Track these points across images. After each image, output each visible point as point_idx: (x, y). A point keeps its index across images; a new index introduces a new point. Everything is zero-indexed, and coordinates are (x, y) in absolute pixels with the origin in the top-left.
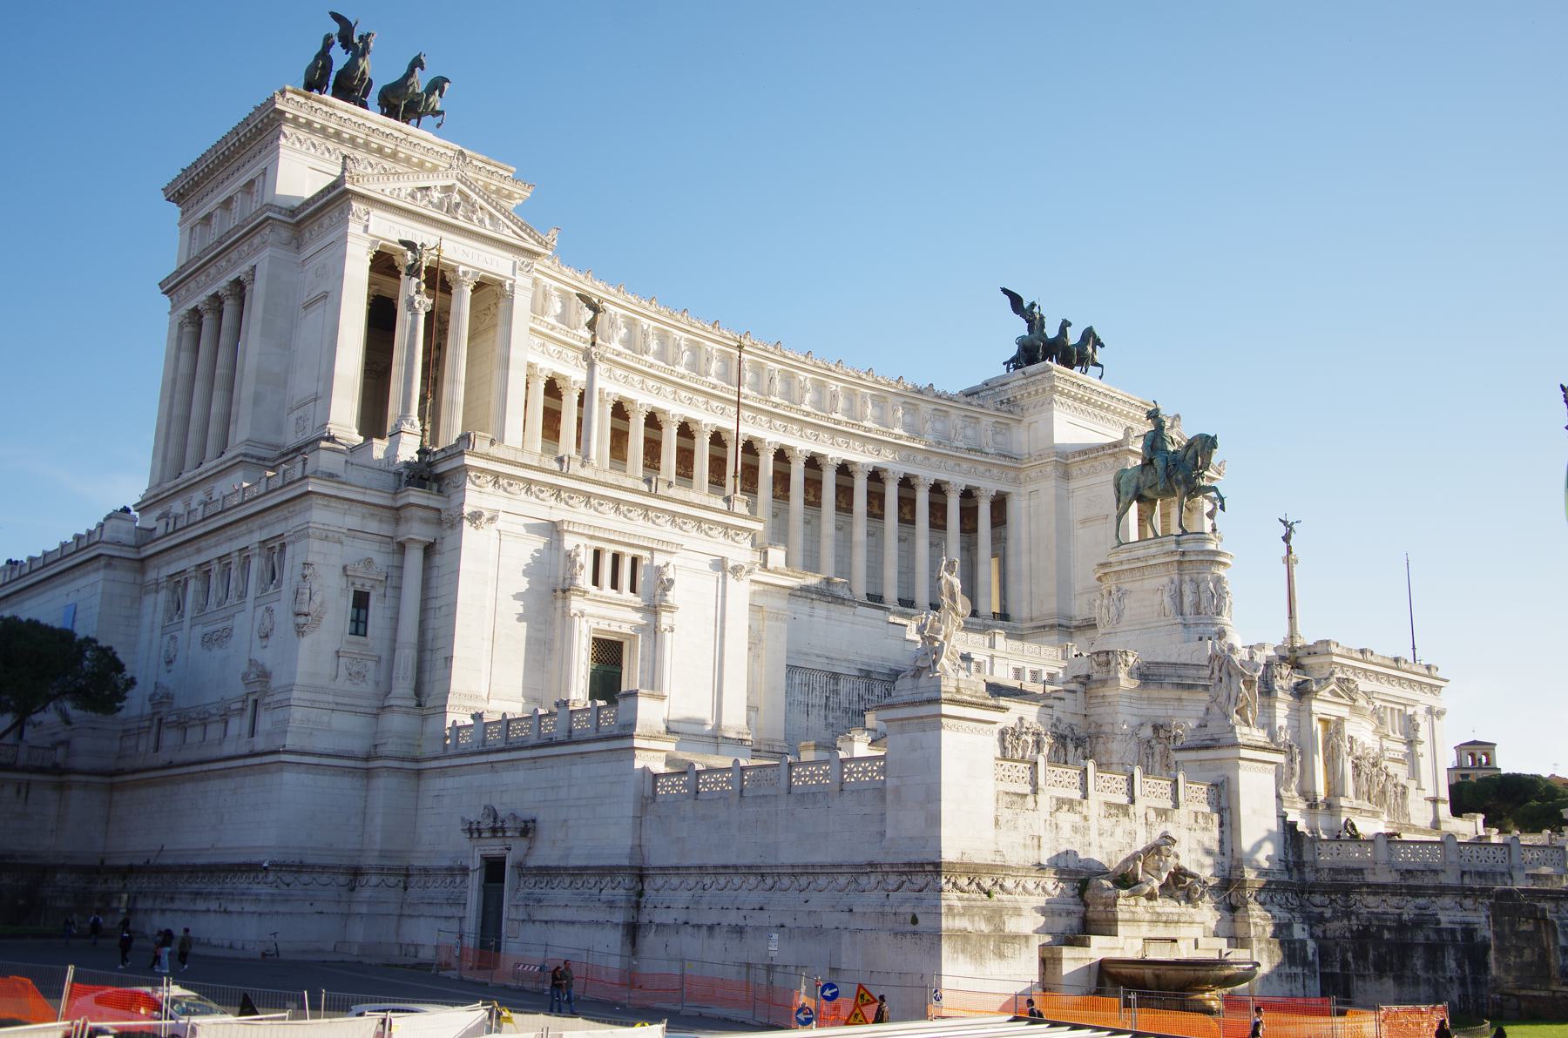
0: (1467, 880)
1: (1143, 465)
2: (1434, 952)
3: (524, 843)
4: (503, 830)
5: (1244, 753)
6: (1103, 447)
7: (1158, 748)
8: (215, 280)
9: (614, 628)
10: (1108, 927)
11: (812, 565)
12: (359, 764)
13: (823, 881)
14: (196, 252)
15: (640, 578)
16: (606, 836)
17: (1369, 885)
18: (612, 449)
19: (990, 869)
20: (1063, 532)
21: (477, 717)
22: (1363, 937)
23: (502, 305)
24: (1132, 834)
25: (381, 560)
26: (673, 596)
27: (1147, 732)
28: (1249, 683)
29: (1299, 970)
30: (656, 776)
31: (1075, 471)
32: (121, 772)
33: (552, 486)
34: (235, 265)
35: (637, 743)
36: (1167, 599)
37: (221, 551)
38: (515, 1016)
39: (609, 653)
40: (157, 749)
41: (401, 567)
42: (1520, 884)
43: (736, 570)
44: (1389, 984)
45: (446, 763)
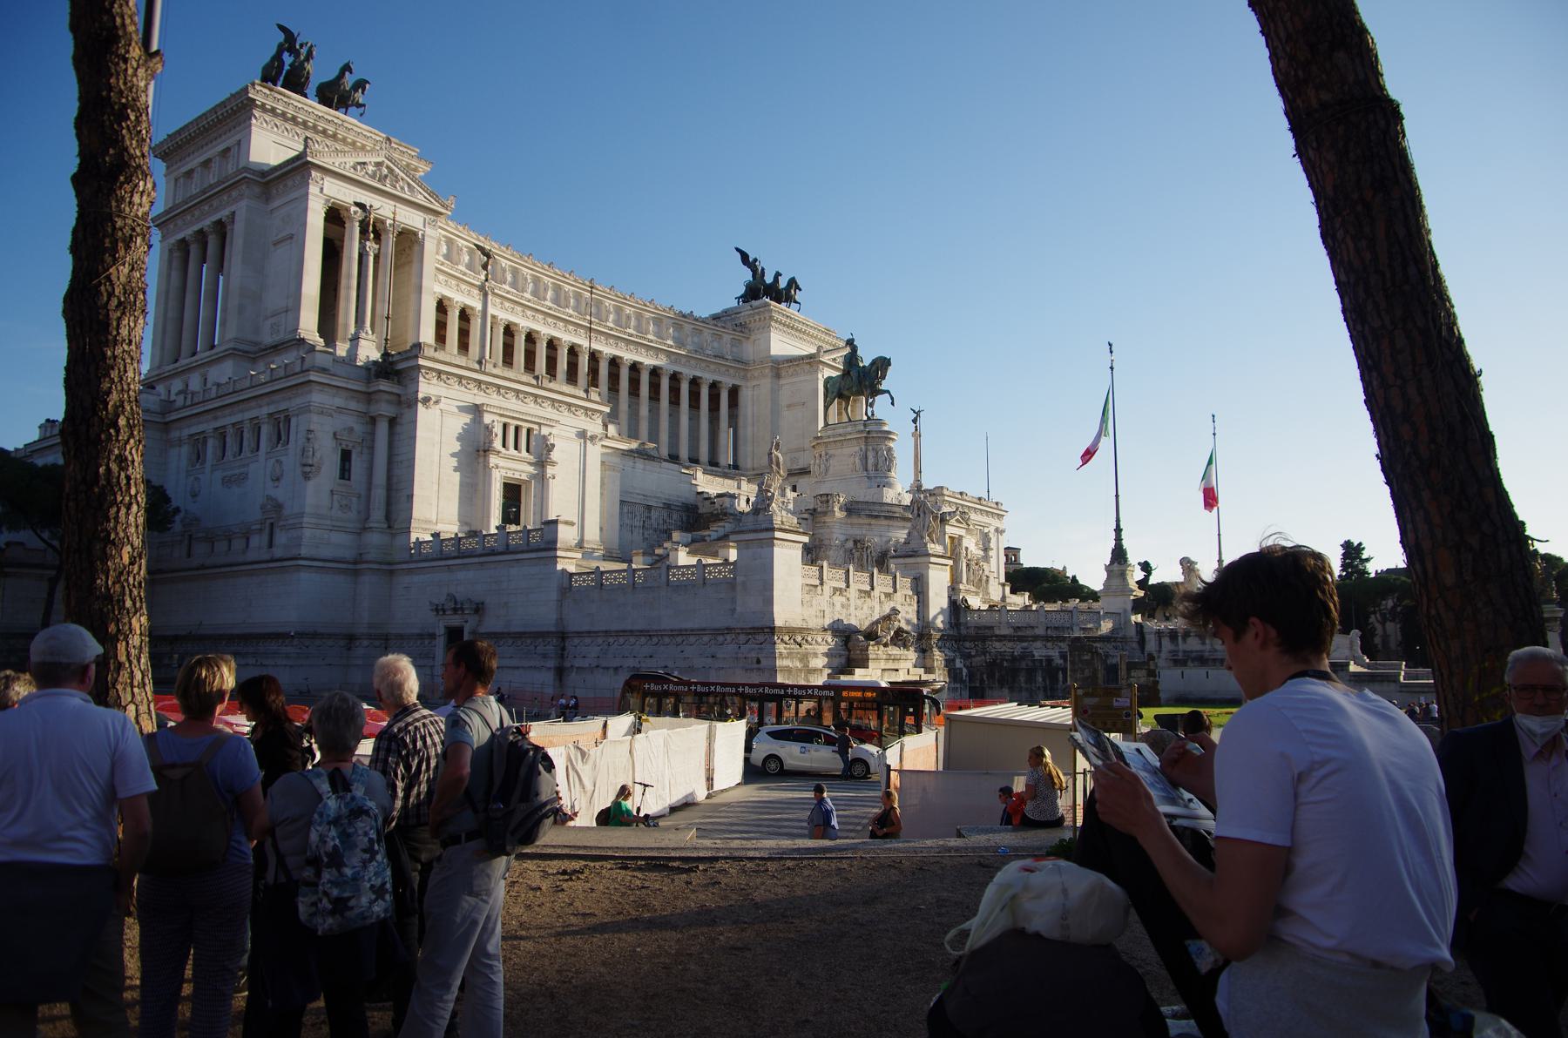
2: (1031, 673)
3: (476, 617)
4: (462, 609)
5: (933, 559)
6: (802, 358)
7: (857, 555)
9: (517, 476)
10: (864, 664)
11: (633, 434)
13: (692, 639)
15: (533, 443)
16: (540, 611)
19: (801, 630)
20: (775, 412)
21: (436, 535)
22: (993, 665)
23: (416, 248)
24: (872, 608)
25: (359, 428)
26: (554, 455)
27: (850, 544)
28: (935, 518)
30: (572, 575)
31: (783, 373)
33: (475, 380)
34: (217, 210)
35: (559, 553)
37: (234, 419)
39: (513, 492)
40: (189, 556)
43: (593, 438)
44: (1006, 691)
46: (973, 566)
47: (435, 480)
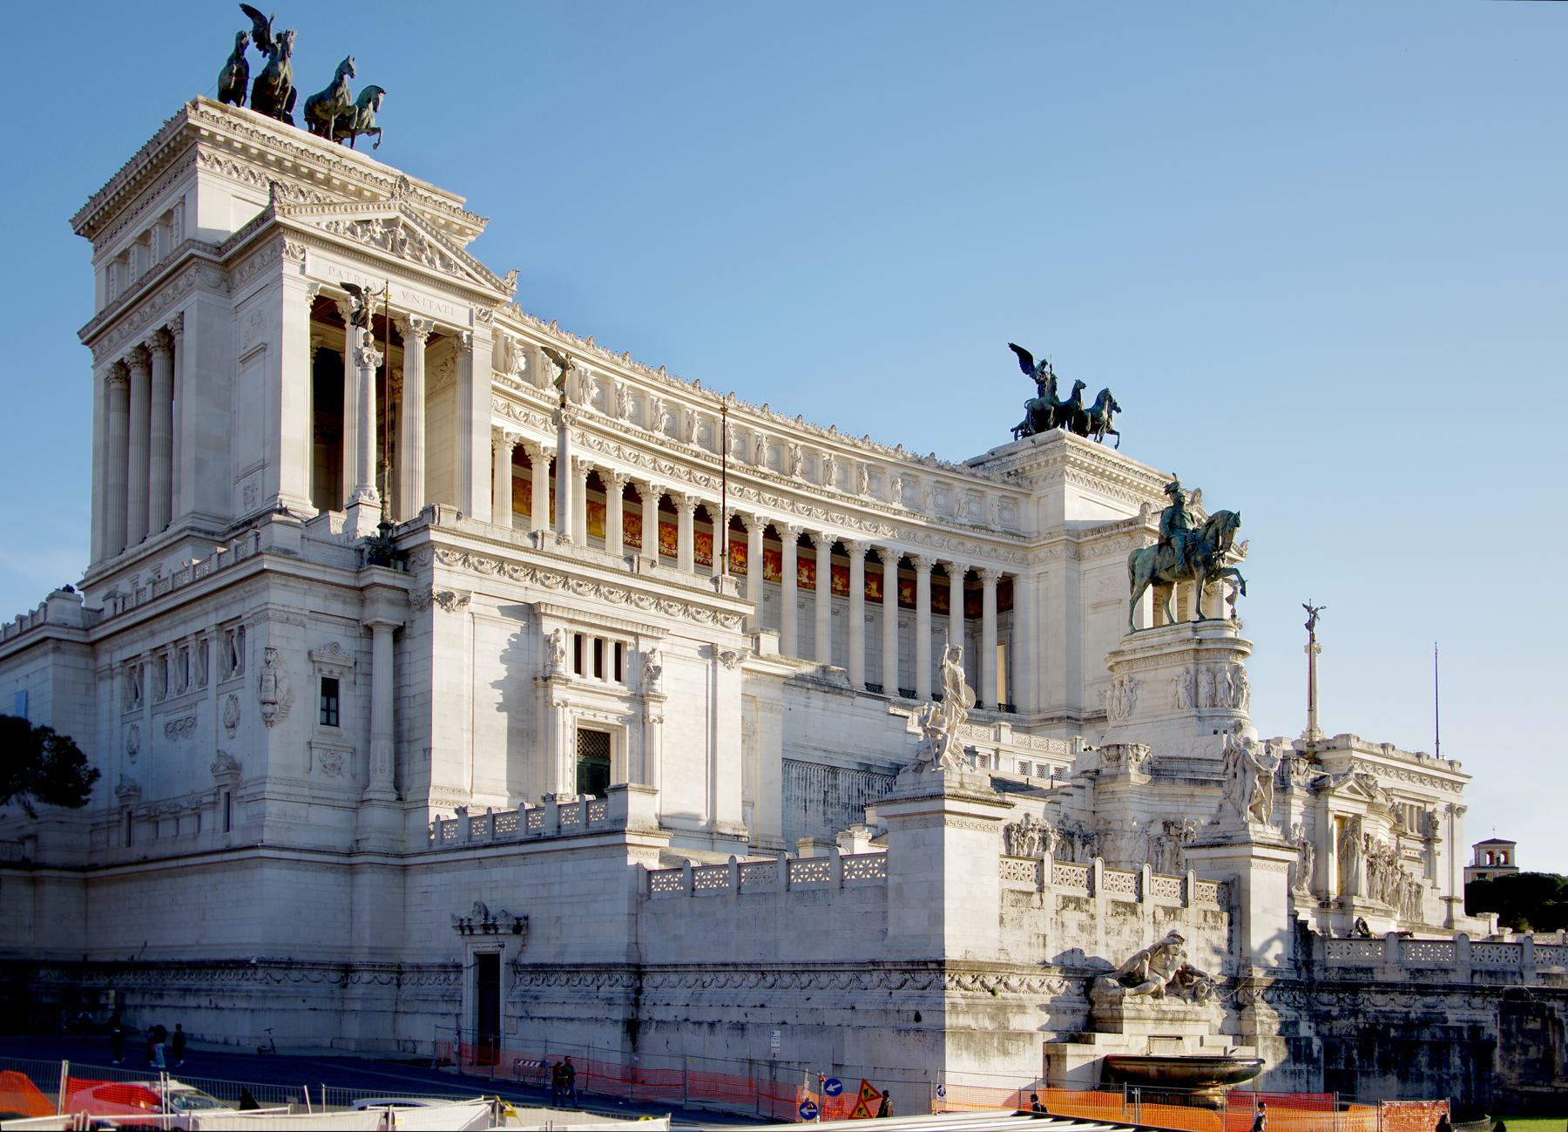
0: (1477, 979)
1: (1160, 546)
2: (1439, 1055)
3: (517, 940)
4: (496, 928)
5: (1257, 851)
8: (139, 329)
12: (342, 860)
14: (115, 296)
15: (625, 666)
16: (604, 934)
17: (1378, 984)
18: (589, 524)
21: (461, 811)
22: (1371, 1036)
23: (460, 359)
25: (349, 644)
26: (661, 685)
29: (1303, 1067)
32: (94, 867)
34: (160, 311)
36: (1181, 690)
38: (518, 1111)
41: (370, 653)
42: (1531, 982)
43: (726, 656)
44: (1392, 1080)
45: (432, 858)
46: (1381, 866)
47: (466, 725)
